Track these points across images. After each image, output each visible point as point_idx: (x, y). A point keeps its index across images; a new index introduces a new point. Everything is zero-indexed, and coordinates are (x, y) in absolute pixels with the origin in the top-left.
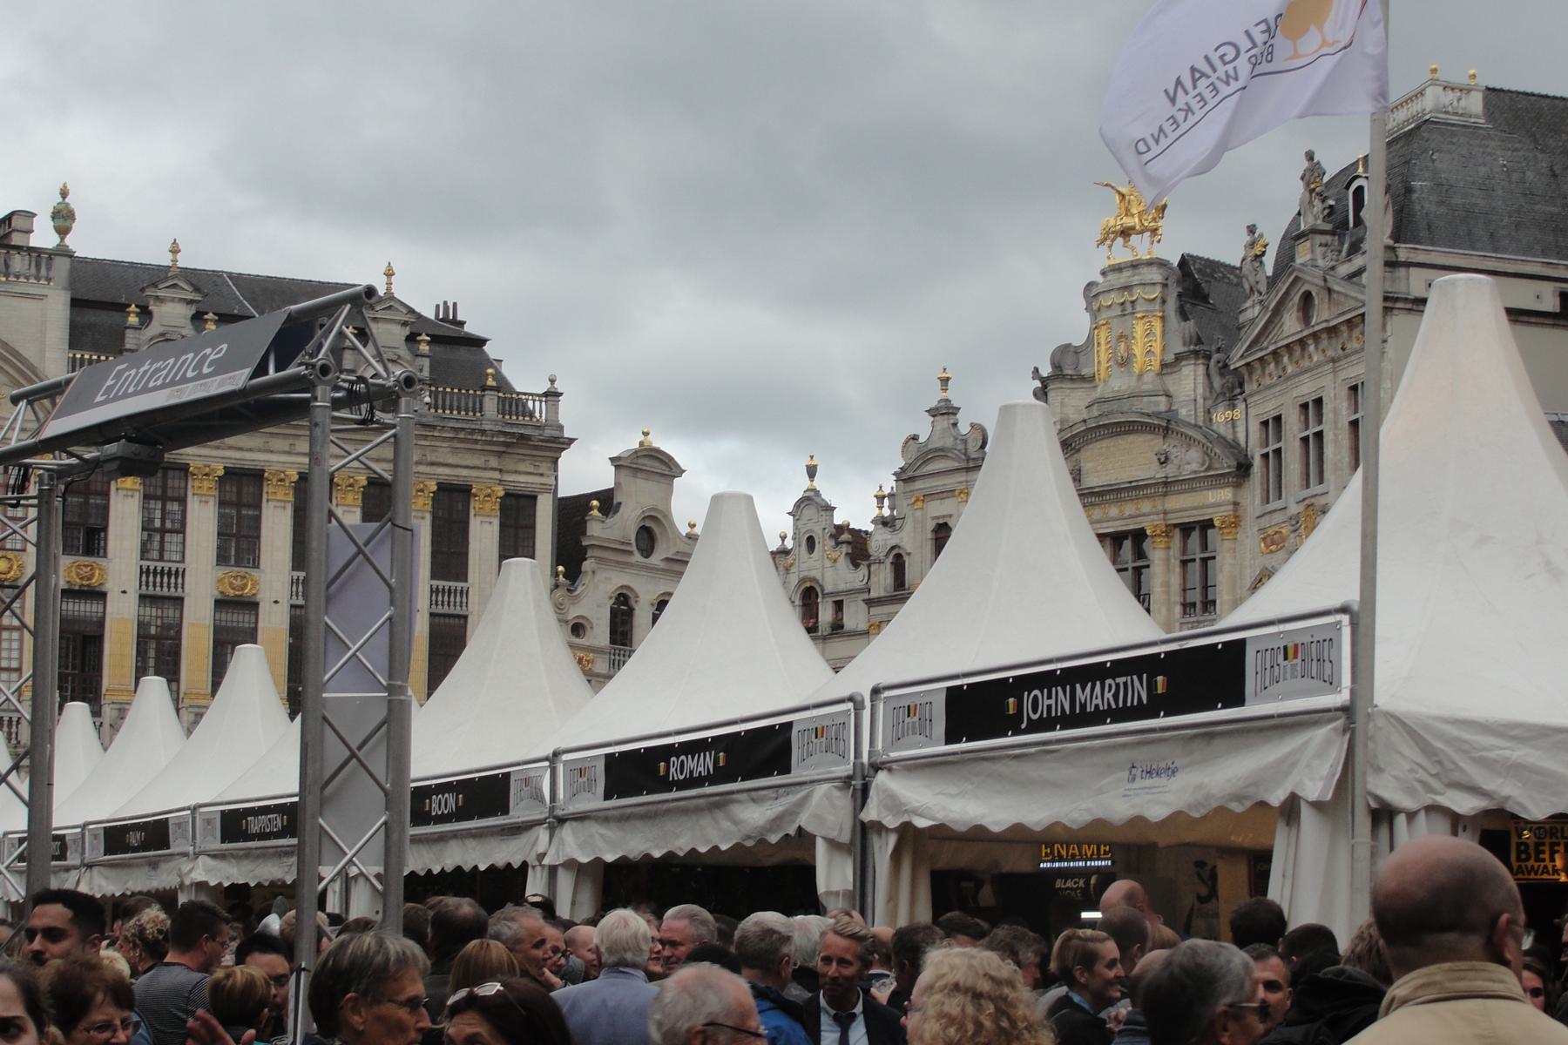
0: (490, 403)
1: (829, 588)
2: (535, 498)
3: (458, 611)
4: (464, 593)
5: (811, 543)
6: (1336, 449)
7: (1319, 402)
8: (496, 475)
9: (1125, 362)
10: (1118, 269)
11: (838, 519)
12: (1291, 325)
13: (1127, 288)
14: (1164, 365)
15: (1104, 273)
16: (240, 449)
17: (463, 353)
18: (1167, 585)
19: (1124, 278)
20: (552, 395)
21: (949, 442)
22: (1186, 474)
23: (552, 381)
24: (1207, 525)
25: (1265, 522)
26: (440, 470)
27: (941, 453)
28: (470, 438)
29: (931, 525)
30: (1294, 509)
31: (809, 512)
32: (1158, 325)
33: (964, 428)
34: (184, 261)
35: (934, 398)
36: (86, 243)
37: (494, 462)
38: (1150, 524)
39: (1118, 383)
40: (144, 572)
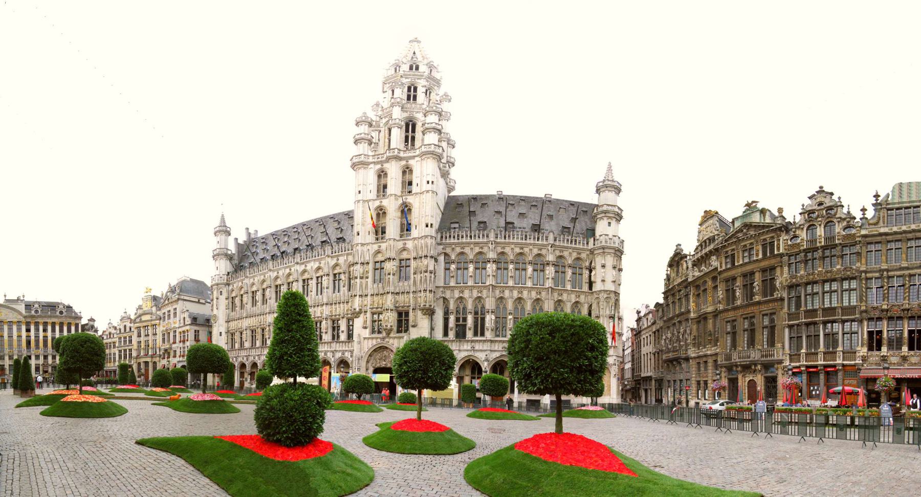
36: (27, 299)
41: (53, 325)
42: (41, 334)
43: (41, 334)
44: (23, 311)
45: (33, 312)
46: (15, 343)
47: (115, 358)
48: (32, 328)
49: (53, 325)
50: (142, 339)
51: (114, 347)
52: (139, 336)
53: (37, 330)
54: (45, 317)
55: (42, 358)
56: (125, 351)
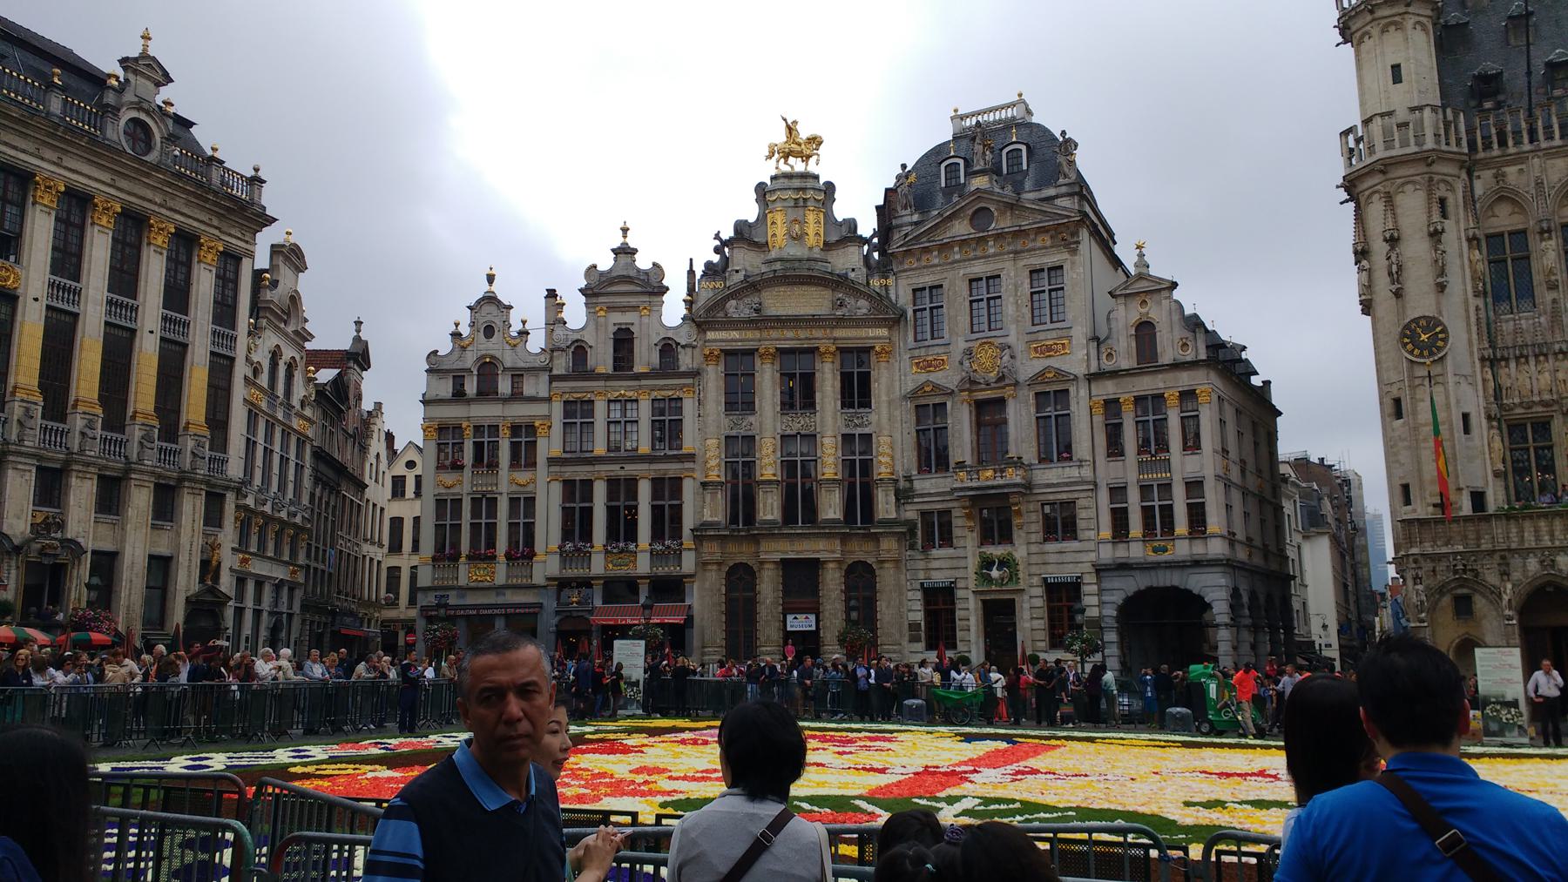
1: (508, 364)
2: (237, 260)
3: (181, 339)
4: (186, 325)
5: (489, 331)
8: (216, 232)
9: (799, 238)
10: (789, 176)
13: (804, 189)
14: (826, 244)
15: (773, 178)
16: (15, 148)
19: (797, 183)
20: (256, 181)
21: (633, 273)
23: (256, 170)
24: (868, 350)
26: (177, 217)
27: (627, 279)
29: (613, 329)
31: (487, 308)
37: (215, 222)
51: (524, 456)
56: (623, 489)
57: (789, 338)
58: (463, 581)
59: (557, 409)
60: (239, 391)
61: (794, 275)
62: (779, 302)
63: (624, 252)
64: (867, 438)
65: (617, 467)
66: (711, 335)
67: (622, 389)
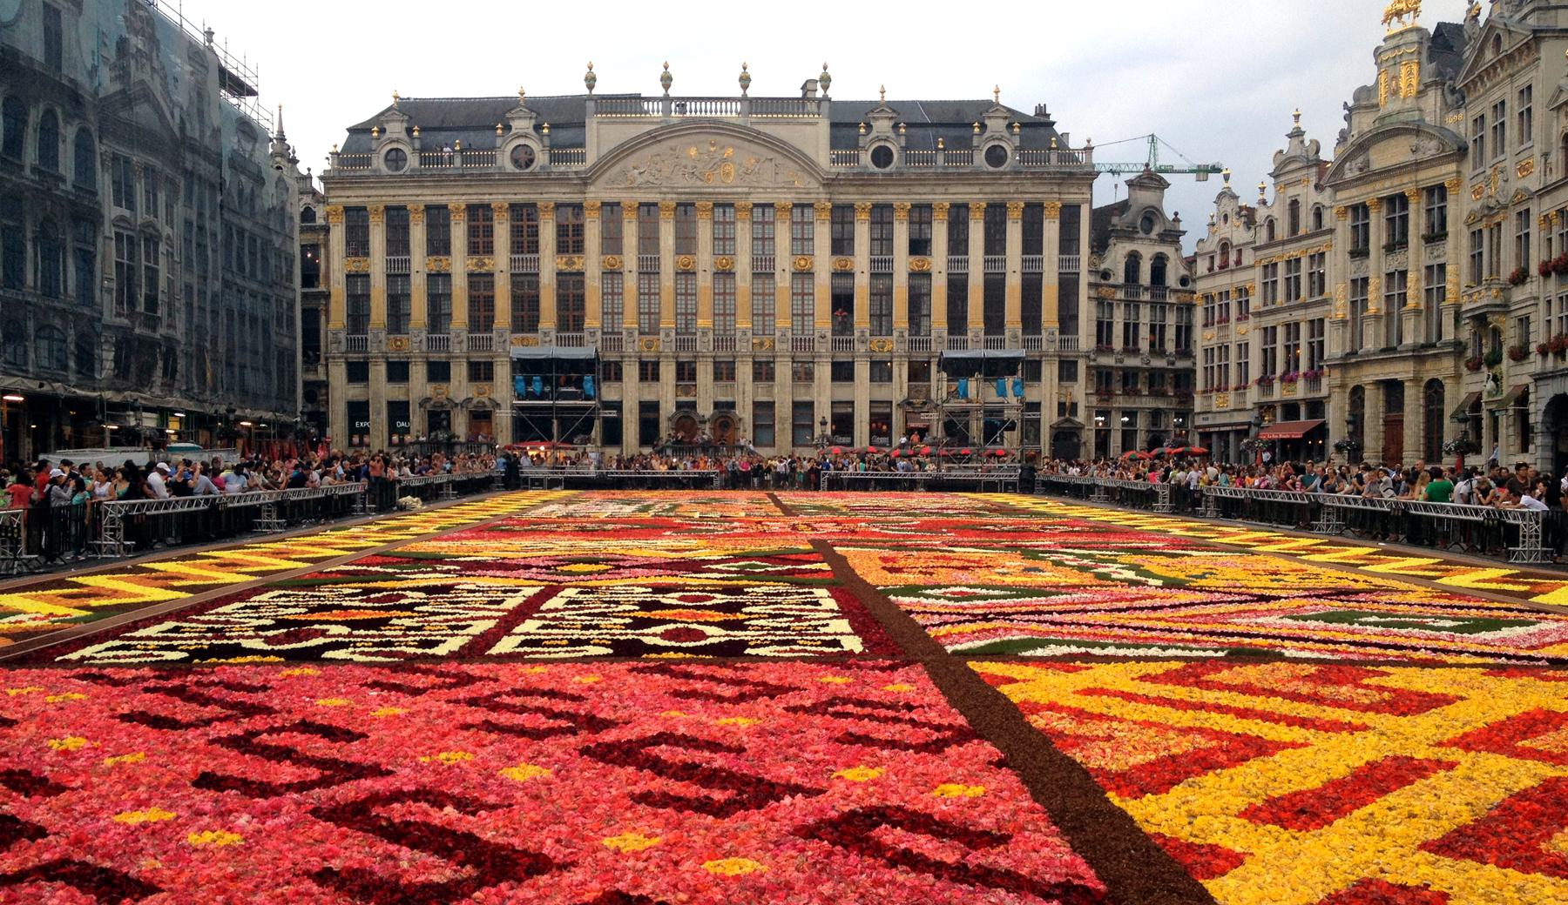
0: (1054, 158)
6: (1511, 132)
7: (1503, 103)
9: (1395, 93)
10: (1393, 36)
11: (1242, 203)
12: (1489, 55)
13: (1398, 47)
17: (1042, 131)
18: (1418, 225)
20: (1089, 149)
22: (1427, 156)
25: (1474, 181)
28: (1039, 178)
29: (1288, 201)
30: (1489, 172)
31: (1225, 201)
32: (1415, 68)
33: (1307, 143)
34: (888, 98)
35: (1290, 127)
36: (837, 93)
38: (1408, 189)
39: (1391, 107)
40: (872, 261)
41: (958, 217)
42: (902, 262)
43: (902, 262)
44: (822, 155)
45: (866, 158)
46: (783, 304)
47: (1243, 367)
48: (862, 233)
49: (958, 217)
50: (1377, 266)
52: (1359, 252)
53: (883, 241)
54: (921, 180)
55: (901, 372)
56: (1293, 329)
57: (1387, 188)
58: (1214, 409)
59: (1258, 273)
60: (1084, 292)
61: (1387, 133)
62: (1382, 157)
63: (1297, 134)
64: (1442, 267)
65: (1286, 315)
66: (1340, 195)
67: (1293, 251)
